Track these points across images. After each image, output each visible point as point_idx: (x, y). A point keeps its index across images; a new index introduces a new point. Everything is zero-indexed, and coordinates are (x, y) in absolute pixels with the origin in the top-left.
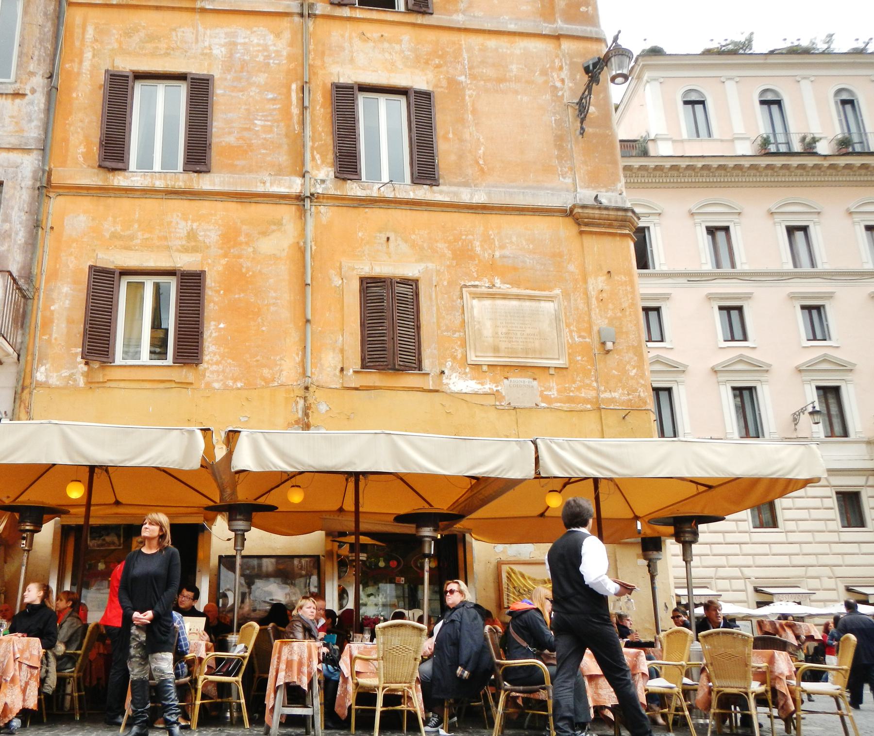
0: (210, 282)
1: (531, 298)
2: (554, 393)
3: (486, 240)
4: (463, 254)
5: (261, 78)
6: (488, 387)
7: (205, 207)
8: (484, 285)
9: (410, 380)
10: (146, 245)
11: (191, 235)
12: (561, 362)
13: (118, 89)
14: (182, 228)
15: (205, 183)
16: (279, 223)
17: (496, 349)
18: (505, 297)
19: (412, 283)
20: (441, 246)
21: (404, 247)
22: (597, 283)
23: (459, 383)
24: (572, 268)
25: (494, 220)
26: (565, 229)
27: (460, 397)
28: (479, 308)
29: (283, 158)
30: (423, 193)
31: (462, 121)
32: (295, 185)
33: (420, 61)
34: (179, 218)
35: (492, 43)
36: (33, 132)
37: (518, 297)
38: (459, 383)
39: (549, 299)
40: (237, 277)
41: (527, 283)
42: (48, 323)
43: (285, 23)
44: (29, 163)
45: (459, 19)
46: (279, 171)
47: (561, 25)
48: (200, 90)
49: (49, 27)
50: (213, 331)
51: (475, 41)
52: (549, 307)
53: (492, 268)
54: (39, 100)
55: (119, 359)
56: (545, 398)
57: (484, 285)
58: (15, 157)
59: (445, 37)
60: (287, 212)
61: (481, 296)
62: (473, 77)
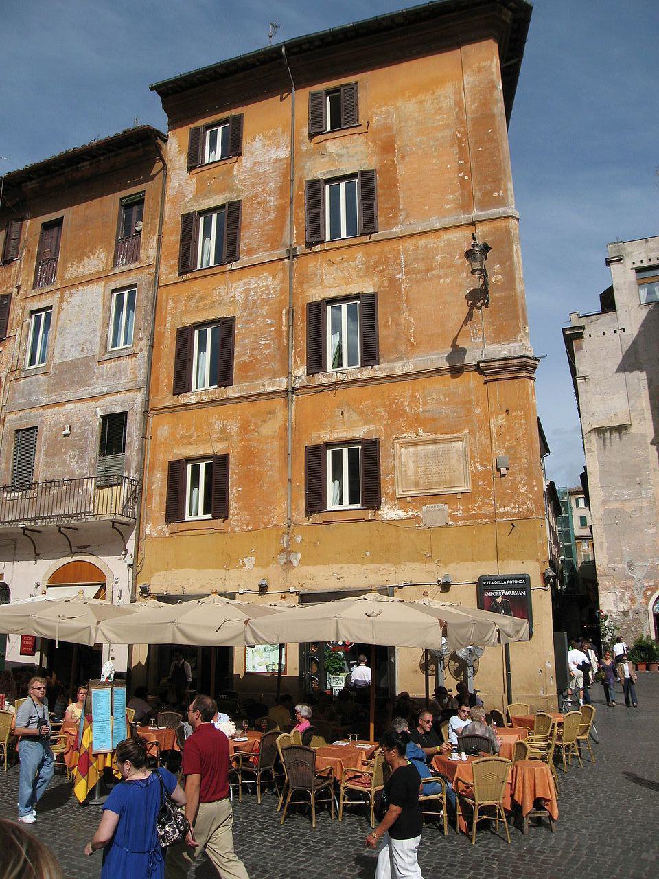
0: (232, 460)
1: (444, 441)
2: (460, 513)
3: (414, 400)
4: (396, 414)
5: (264, 311)
6: (412, 513)
7: (231, 408)
8: (411, 436)
10: (200, 441)
11: (223, 430)
12: (467, 488)
13: (184, 336)
14: (218, 425)
15: (231, 392)
16: (273, 413)
17: (417, 484)
18: (425, 443)
20: (381, 410)
21: (354, 416)
22: (498, 420)
24: (478, 411)
27: (390, 523)
28: (406, 454)
29: (275, 365)
30: (368, 372)
31: (398, 309)
32: (282, 383)
33: (369, 271)
34: (215, 419)
35: (422, 242)
36: (142, 376)
37: (435, 442)
39: (458, 440)
40: (249, 455)
41: (441, 428)
42: (150, 496)
43: (279, 265)
44: (140, 397)
45: (398, 230)
46: (275, 375)
47: (477, 213)
48: (225, 328)
49: (149, 307)
50: (234, 493)
51: (409, 244)
52: (458, 446)
53: (417, 422)
54: (145, 354)
55: (187, 518)
56: (454, 518)
57: (411, 436)
58: (132, 394)
59: (387, 247)
60: (278, 404)
61: (406, 445)
62: (408, 273)
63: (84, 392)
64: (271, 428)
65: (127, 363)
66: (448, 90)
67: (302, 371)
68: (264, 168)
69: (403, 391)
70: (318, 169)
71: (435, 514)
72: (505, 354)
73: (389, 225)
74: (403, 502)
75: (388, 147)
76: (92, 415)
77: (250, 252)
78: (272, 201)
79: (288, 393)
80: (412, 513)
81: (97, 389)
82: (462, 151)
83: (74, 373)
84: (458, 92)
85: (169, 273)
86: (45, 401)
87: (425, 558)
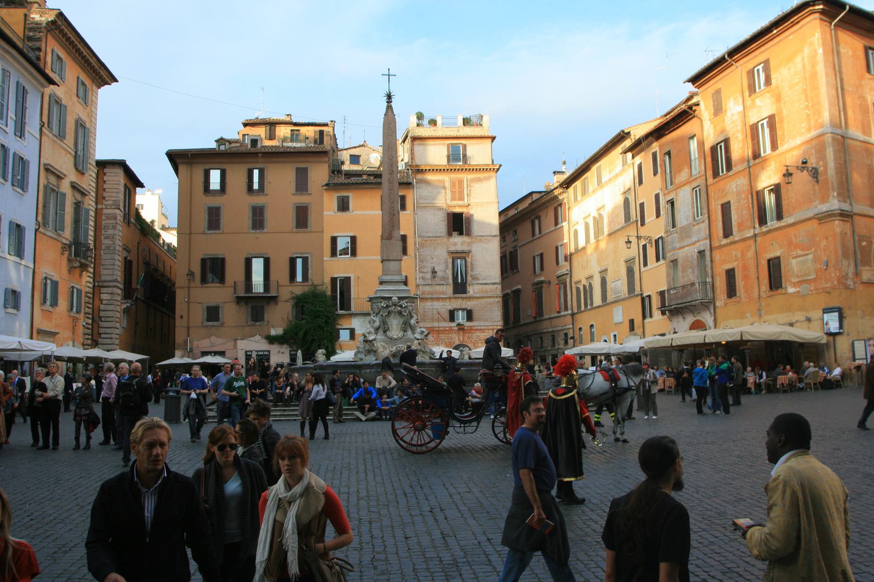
2: (812, 288)
3: (795, 236)
4: (790, 243)
5: (743, 196)
6: (797, 289)
9: (780, 291)
14: (734, 253)
16: (750, 246)
18: (800, 256)
19: (778, 258)
22: (824, 243)
23: (791, 290)
25: (797, 226)
26: (815, 223)
27: (791, 294)
29: (749, 224)
32: (750, 233)
37: (803, 256)
38: (791, 290)
40: (745, 267)
44: (708, 241)
52: (811, 256)
53: (797, 246)
54: (707, 221)
56: (811, 290)
61: (794, 258)
63: (690, 241)
64: (751, 254)
65: (702, 225)
66: (798, 59)
67: (757, 226)
68: (736, 117)
69: (791, 231)
70: (753, 120)
71: (804, 289)
72: (824, 209)
73: (782, 145)
74: (795, 285)
75: (778, 99)
76: (693, 251)
77: (736, 166)
78: (740, 136)
79: (755, 236)
80: (797, 289)
81: (694, 239)
82: (806, 95)
83: (686, 232)
84: (803, 60)
85: (710, 180)
86: (678, 246)
87: (802, 309)
